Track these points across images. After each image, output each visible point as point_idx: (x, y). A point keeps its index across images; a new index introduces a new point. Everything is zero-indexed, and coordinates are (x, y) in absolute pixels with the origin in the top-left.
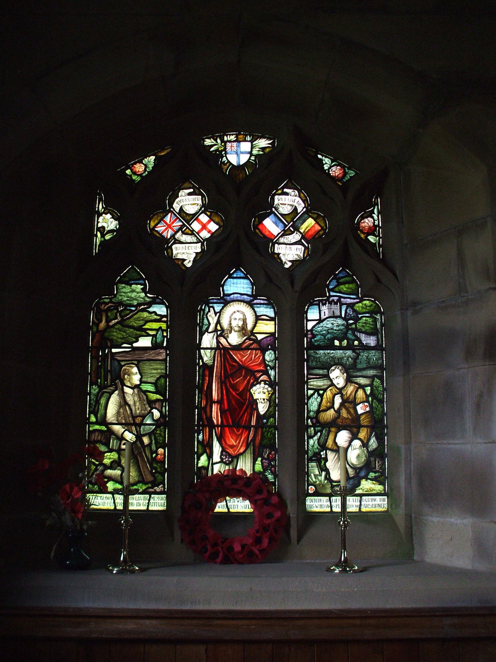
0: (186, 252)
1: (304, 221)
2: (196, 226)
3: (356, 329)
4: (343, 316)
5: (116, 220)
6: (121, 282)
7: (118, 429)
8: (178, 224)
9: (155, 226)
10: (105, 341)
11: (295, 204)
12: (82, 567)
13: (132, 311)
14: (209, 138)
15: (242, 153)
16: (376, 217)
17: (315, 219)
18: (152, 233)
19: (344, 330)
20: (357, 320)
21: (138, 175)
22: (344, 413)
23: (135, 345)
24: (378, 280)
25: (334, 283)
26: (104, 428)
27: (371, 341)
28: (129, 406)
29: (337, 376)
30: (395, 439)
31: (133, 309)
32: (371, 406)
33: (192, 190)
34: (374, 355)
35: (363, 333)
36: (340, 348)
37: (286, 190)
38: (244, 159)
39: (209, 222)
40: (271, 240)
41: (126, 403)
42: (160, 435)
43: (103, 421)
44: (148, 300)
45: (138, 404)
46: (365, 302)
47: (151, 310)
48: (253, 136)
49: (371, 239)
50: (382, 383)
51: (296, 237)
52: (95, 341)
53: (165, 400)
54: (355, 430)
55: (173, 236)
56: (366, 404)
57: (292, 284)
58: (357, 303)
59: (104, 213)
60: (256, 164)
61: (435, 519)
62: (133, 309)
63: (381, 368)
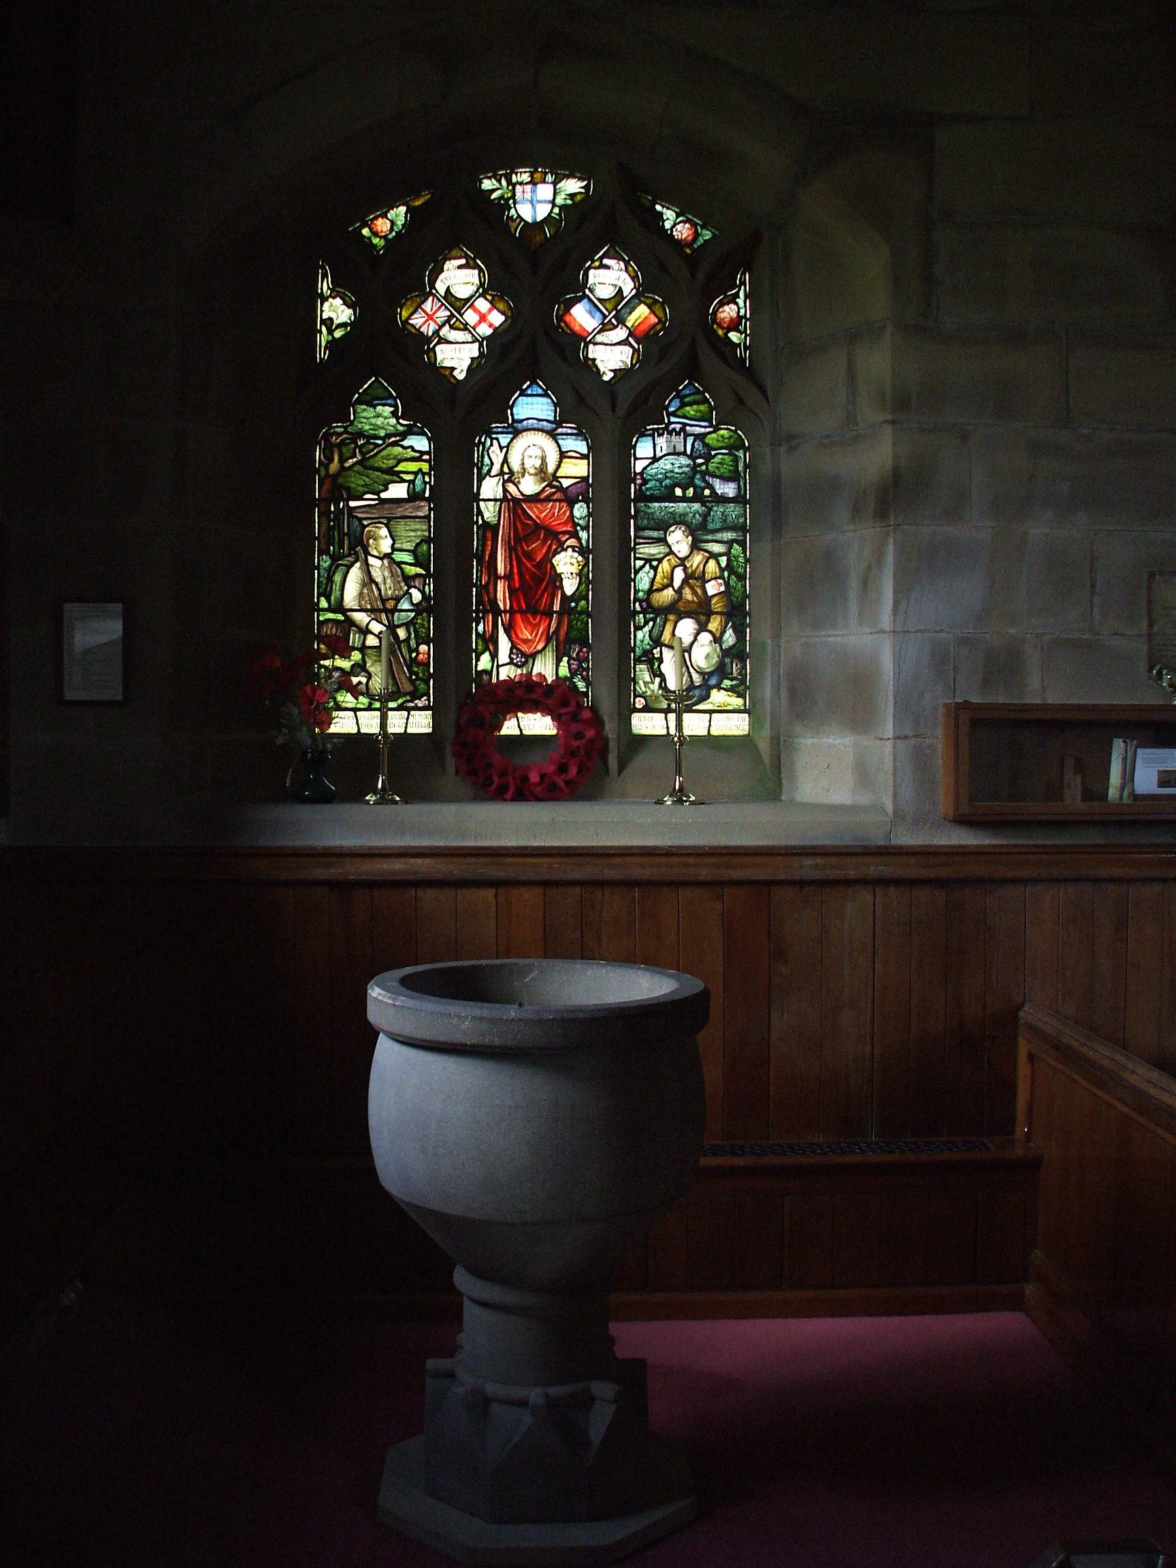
0: (457, 356)
1: (633, 309)
2: (470, 317)
3: (707, 472)
4: (689, 452)
5: (349, 307)
6: (359, 402)
7: (361, 618)
8: (443, 314)
9: (409, 318)
10: (339, 490)
11: (620, 284)
12: (326, 798)
13: (377, 445)
14: (490, 178)
15: (540, 202)
16: (741, 303)
17: (649, 307)
18: (404, 328)
19: (690, 474)
20: (708, 458)
21: (381, 237)
22: (688, 594)
23: (383, 495)
24: (741, 401)
25: (676, 403)
26: (340, 617)
27: (729, 490)
28: (377, 584)
29: (679, 540)
30: (758, 632)
31: (380, 442)
32: (727, 584)
33: (463, 261)
34: (733, 510)
35: (717, 477)
36: (684, 499)
37: (605, 261)
38: (542, 212)
39: (490, 311)
40: (581, 339)
41: (372, 580)
42: (423, 626)
43: (339, 607)
44: (401, 428)
45: (389, 581)
46: (722, 432)
47: (405, 443)
48: (557, 175)
49: (734, 337)
50: (744, 552)
51: (620, 334)
52: (324, 488)
53: (428, 575)
54: (703, 618)
55: (436, 333)
56: (720, 581)
57: (614, 406)
58: (710, 433)
59: (330, 296)
60: (561, 220)
61: (809, 741)
62: (380, 442)
63: (742, 529)
